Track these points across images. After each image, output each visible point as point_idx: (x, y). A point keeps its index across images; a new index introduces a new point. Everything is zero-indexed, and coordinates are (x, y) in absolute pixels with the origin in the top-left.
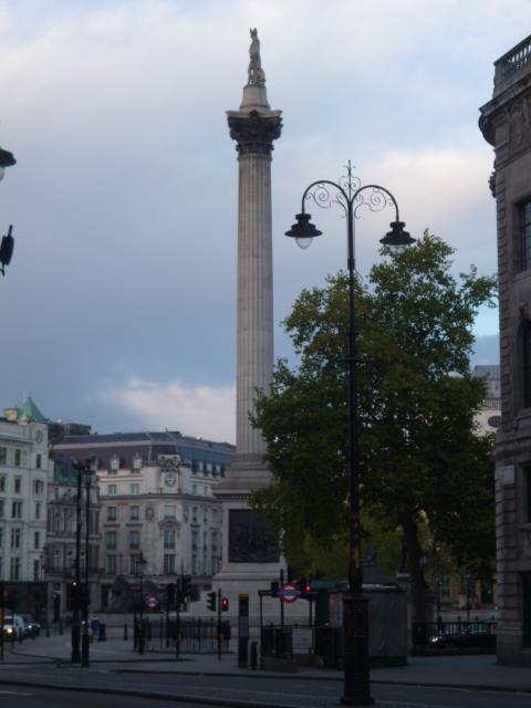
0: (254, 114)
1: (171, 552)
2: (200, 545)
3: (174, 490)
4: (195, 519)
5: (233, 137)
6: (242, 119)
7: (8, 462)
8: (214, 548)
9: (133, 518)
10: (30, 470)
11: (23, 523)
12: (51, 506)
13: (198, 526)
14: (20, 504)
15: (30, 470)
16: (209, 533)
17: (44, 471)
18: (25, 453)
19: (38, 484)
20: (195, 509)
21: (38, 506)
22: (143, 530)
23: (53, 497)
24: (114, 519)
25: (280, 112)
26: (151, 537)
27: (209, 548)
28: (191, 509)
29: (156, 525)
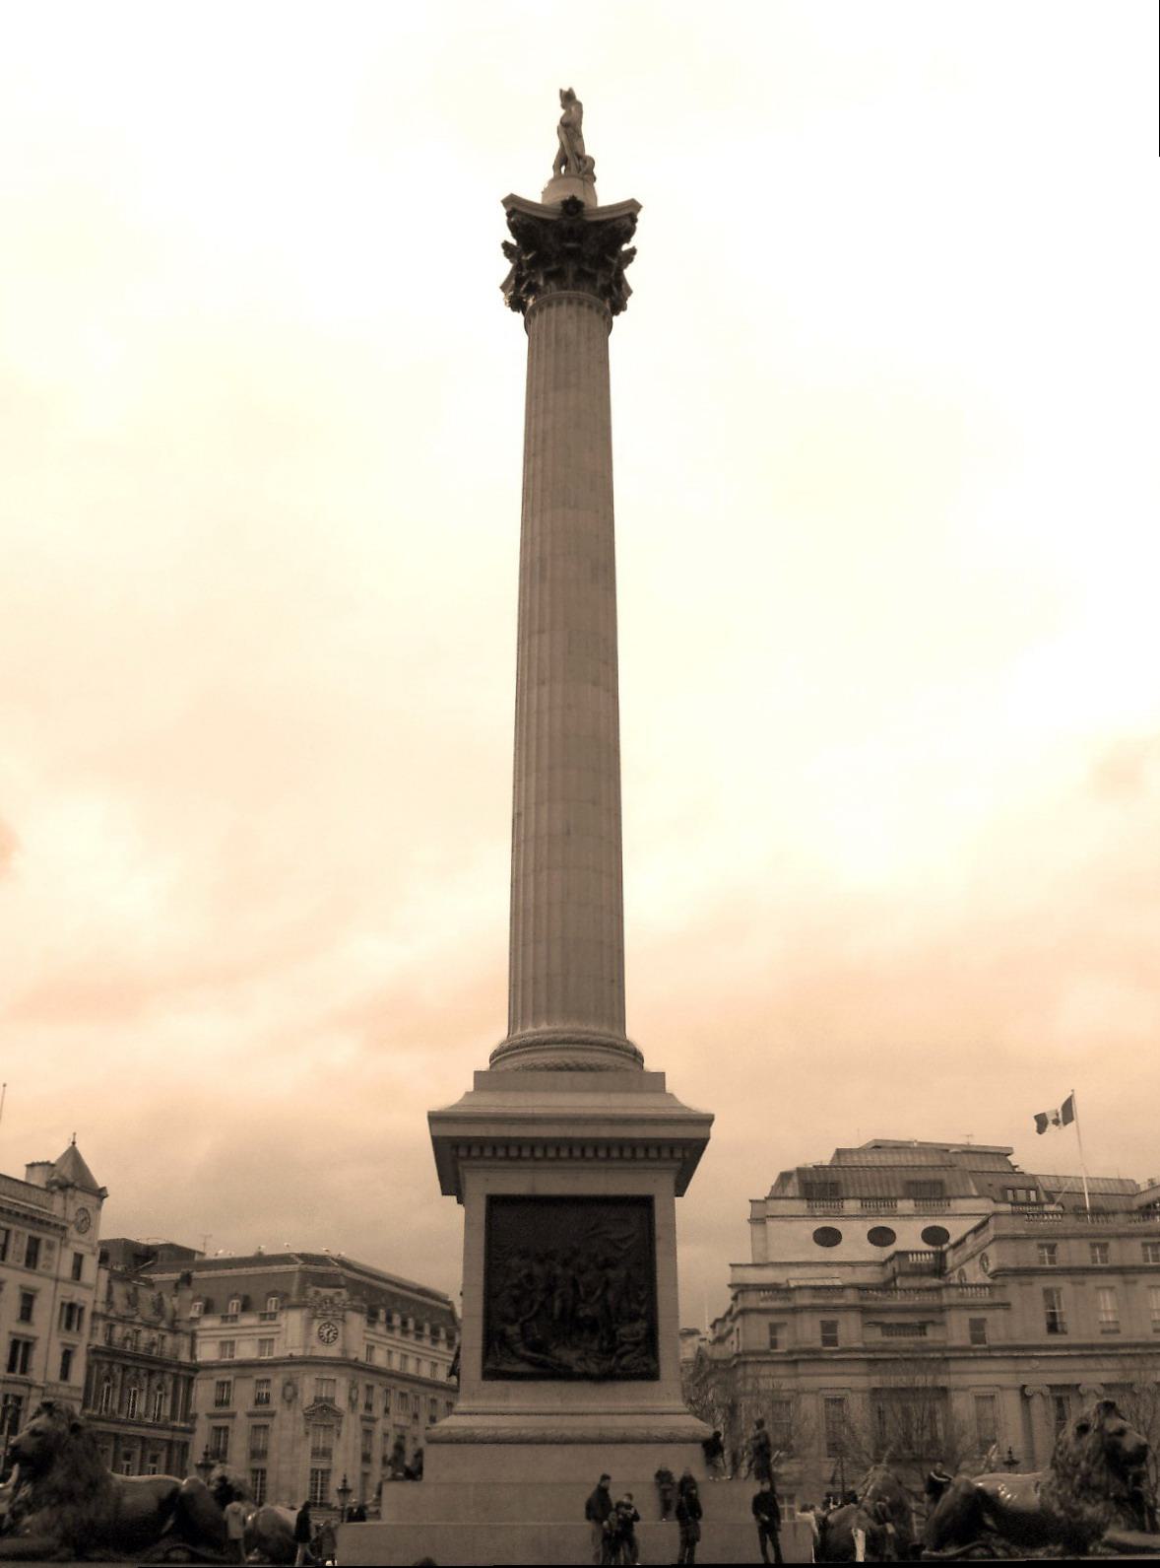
0: (573, 206)
1: (322, 1465)
3: (333, 1351)
4: (369, 1407)
6: (544, 222)
9: (258, 1402)
10: (57, 1280)
11: (30, 1386)
12: (92, 1357)
13: (373, 1420)
14: (28, 1346)
15: (57, 1280)
17: (88, 1287)
18: (50, 1246)
19: (71, 1313)
20: (369, 1388)
21: (67, 1355)
22: (274, 1424)
23: (100, 1341)
24: (227, 1403)
26: (288, 1434)
28: (362, 1388)
29: (300, 1414)
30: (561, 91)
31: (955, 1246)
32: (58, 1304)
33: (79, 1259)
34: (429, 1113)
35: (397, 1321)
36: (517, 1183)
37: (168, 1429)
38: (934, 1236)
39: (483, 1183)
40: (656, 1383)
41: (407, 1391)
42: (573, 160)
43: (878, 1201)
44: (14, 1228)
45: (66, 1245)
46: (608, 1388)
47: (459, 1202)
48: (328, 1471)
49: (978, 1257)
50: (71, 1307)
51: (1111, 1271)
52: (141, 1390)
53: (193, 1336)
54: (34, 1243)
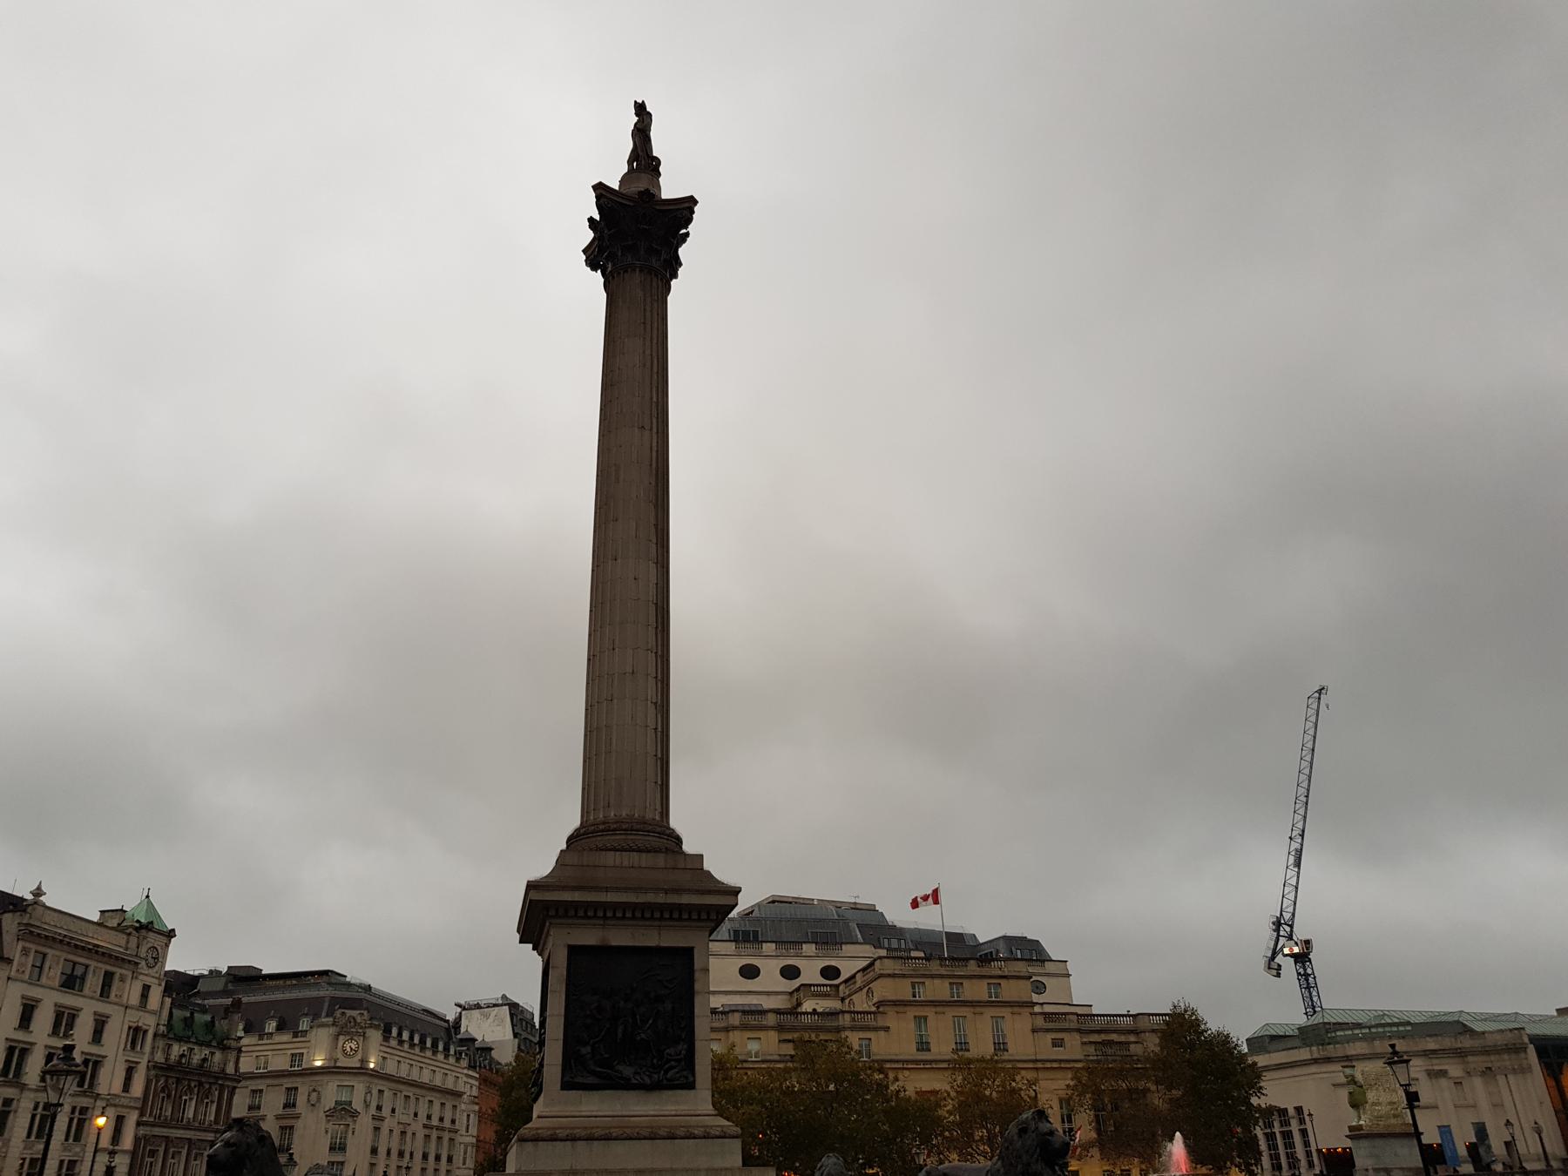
2: (382, 1150)
4: (379, 1108)
5: (592, 263)
7: (86, 991)
8: (401, 1154)
9: (286, 1106)
13: (382, 1119)
16: (396, 1133)
18: (122, 979)
19: (136, 1034)
20: (381, 1091)
21: (130, 1072)
22: (299, 1125)
25: (696, 202)
27: (394, 1153)
28: (375, 1092)
29: (322, 1115)
30: (635, 102)
31: (846, 981)
32: (126, 1028)
33: (146, 988)
34: (528, 882)
35: (406, 1036)
36: (588, 937)
37: (211, 1132)
38: (830, 972)
39: (561, 938)
40: (693, 1091)
41: (411, 1094)
42: (644, 160)
43: (788, 944)
44: (93, 964)
45: (136, 978)
46: (655, 1095)
47: (534, 949)
48: (342, 1163)
49: (865, 990)
50: (137, 1029)
51: (965, 1003)
52: (212, 1102)
53: (240, 1051)
54: (109, 977)
